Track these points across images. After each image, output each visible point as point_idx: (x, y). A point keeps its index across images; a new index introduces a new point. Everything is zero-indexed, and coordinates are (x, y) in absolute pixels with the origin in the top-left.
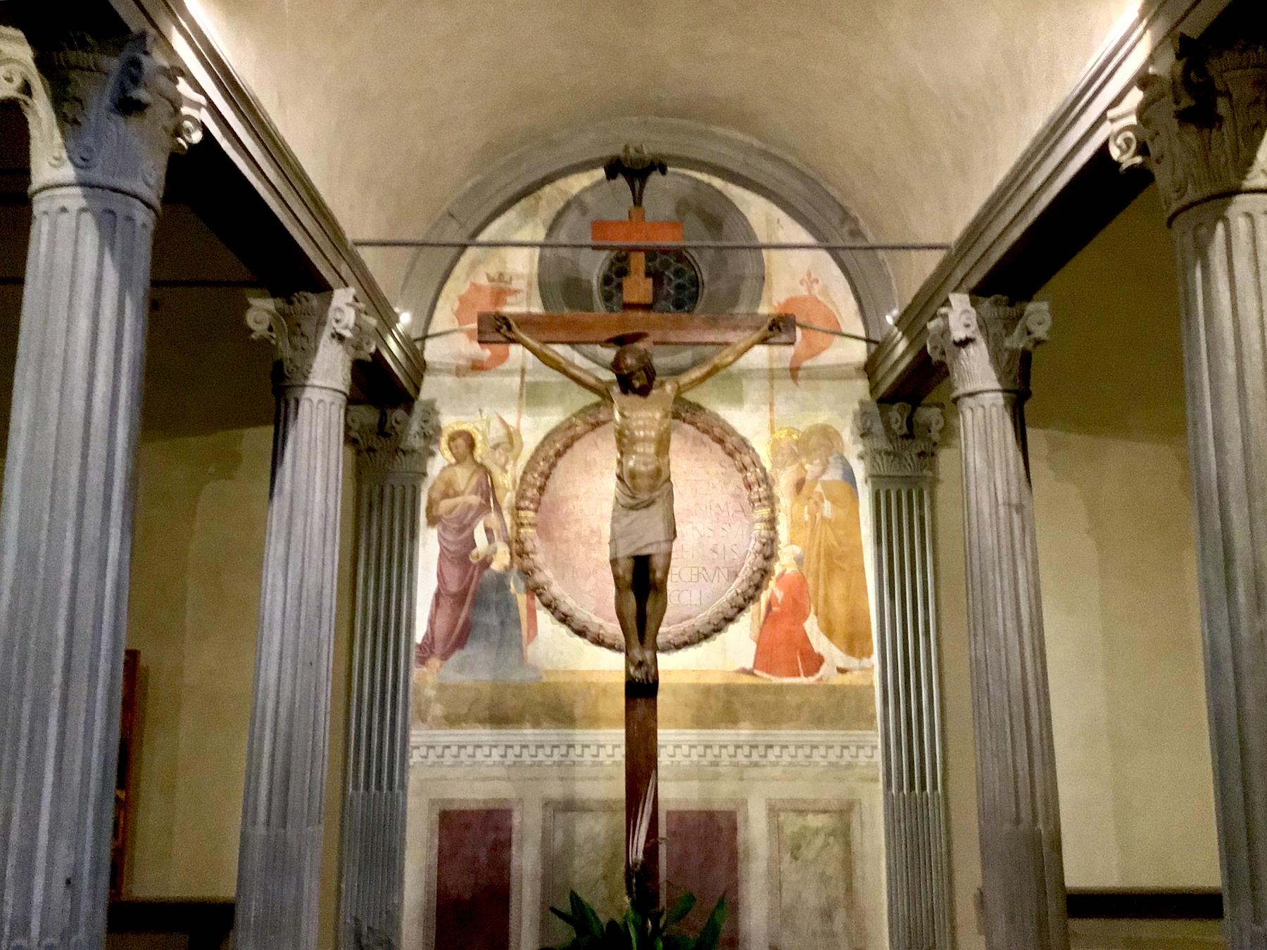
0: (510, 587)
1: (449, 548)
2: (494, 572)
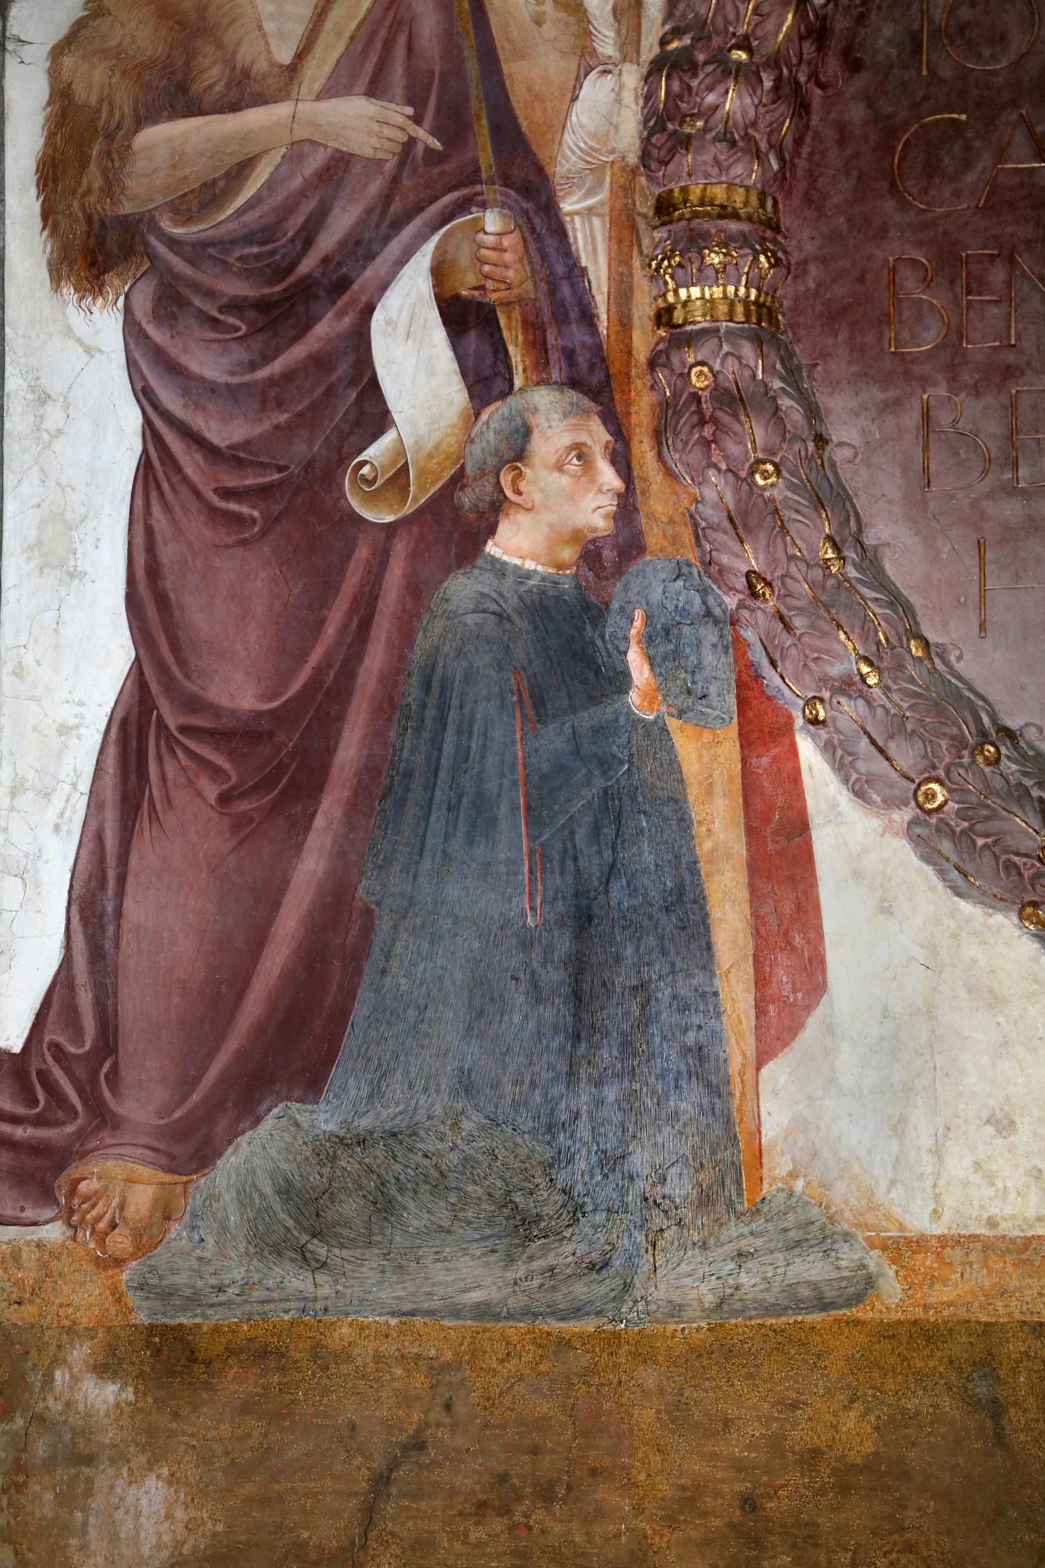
0: (622, 680)
1: (199, 422)
2: (500, 569)
